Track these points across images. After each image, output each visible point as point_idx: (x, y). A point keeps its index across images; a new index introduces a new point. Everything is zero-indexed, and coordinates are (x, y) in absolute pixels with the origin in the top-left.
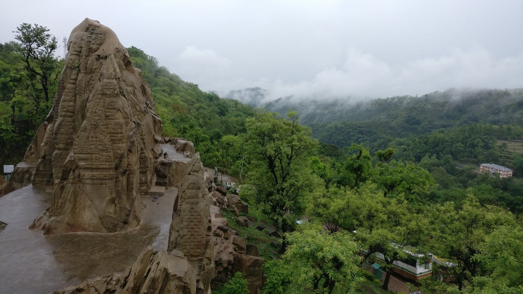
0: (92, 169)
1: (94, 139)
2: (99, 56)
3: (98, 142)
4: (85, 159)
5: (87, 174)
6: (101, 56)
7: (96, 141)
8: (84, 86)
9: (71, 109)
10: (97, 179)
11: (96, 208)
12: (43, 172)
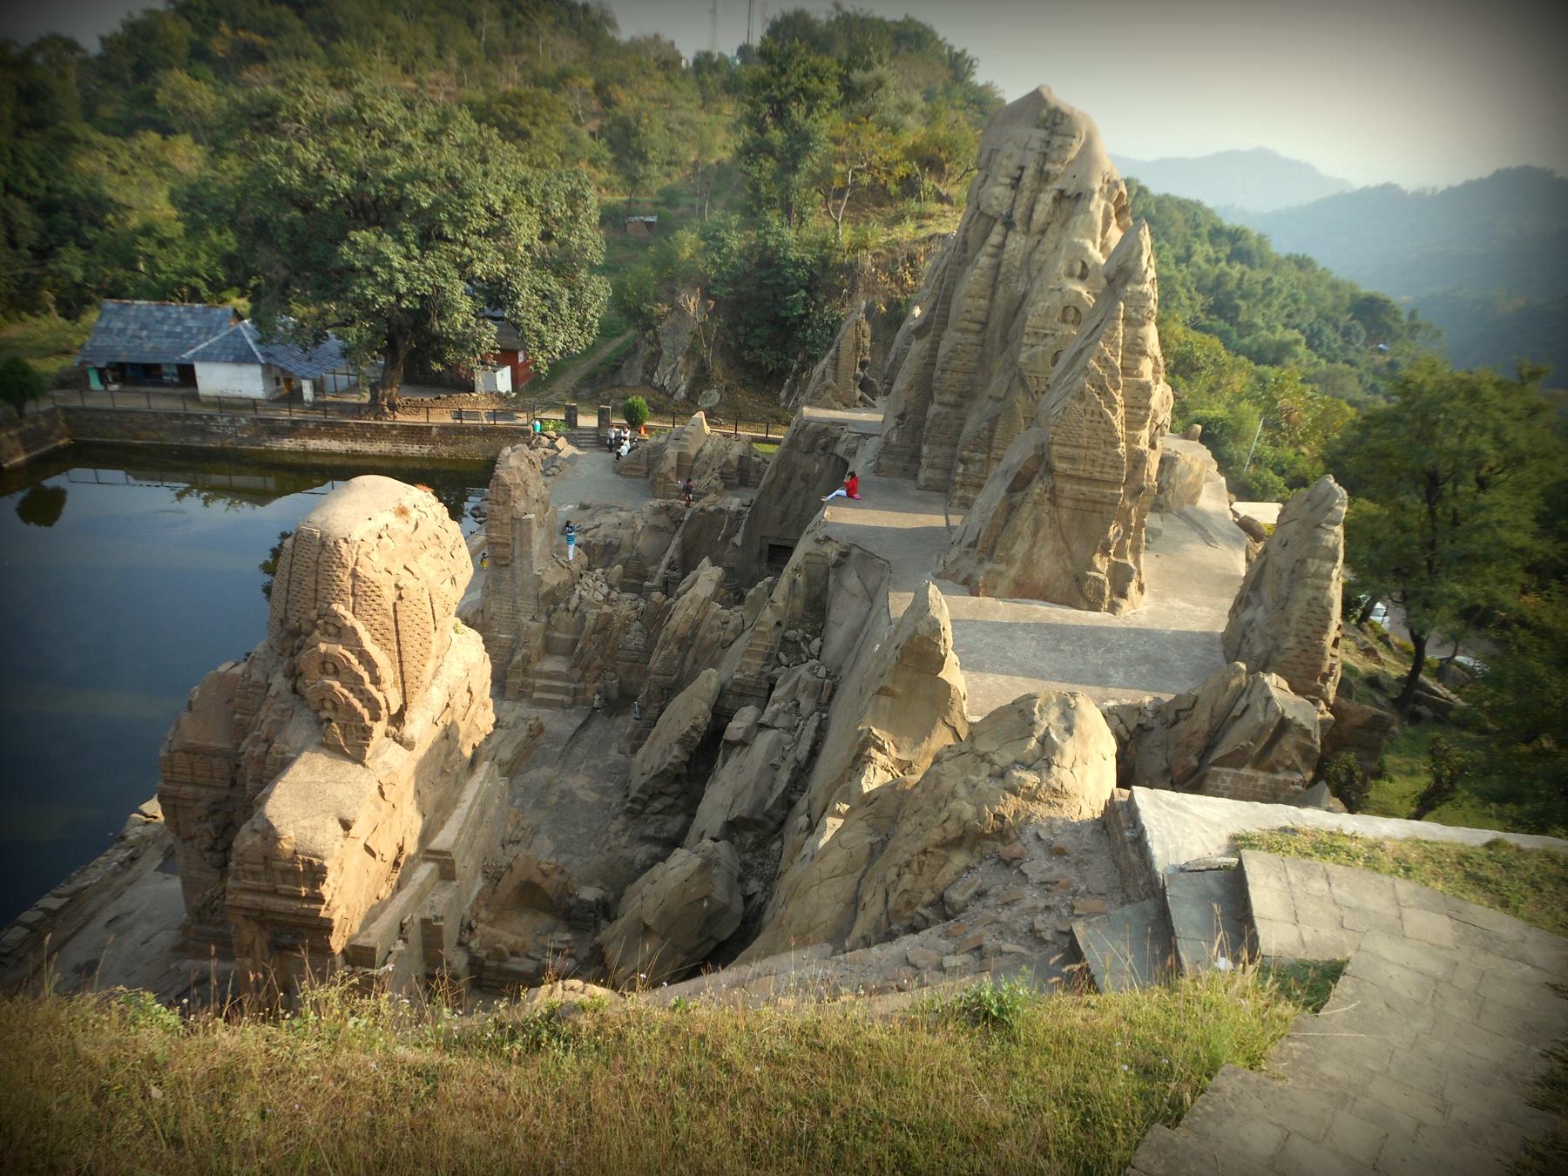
0: (1079, 480)
1: (1096, 418)
2: (1061, 192)
5: (1068, 488)
6: (1068, 193)
8: (1017, 264)
9: (980, 316)
11: (1071, 558)
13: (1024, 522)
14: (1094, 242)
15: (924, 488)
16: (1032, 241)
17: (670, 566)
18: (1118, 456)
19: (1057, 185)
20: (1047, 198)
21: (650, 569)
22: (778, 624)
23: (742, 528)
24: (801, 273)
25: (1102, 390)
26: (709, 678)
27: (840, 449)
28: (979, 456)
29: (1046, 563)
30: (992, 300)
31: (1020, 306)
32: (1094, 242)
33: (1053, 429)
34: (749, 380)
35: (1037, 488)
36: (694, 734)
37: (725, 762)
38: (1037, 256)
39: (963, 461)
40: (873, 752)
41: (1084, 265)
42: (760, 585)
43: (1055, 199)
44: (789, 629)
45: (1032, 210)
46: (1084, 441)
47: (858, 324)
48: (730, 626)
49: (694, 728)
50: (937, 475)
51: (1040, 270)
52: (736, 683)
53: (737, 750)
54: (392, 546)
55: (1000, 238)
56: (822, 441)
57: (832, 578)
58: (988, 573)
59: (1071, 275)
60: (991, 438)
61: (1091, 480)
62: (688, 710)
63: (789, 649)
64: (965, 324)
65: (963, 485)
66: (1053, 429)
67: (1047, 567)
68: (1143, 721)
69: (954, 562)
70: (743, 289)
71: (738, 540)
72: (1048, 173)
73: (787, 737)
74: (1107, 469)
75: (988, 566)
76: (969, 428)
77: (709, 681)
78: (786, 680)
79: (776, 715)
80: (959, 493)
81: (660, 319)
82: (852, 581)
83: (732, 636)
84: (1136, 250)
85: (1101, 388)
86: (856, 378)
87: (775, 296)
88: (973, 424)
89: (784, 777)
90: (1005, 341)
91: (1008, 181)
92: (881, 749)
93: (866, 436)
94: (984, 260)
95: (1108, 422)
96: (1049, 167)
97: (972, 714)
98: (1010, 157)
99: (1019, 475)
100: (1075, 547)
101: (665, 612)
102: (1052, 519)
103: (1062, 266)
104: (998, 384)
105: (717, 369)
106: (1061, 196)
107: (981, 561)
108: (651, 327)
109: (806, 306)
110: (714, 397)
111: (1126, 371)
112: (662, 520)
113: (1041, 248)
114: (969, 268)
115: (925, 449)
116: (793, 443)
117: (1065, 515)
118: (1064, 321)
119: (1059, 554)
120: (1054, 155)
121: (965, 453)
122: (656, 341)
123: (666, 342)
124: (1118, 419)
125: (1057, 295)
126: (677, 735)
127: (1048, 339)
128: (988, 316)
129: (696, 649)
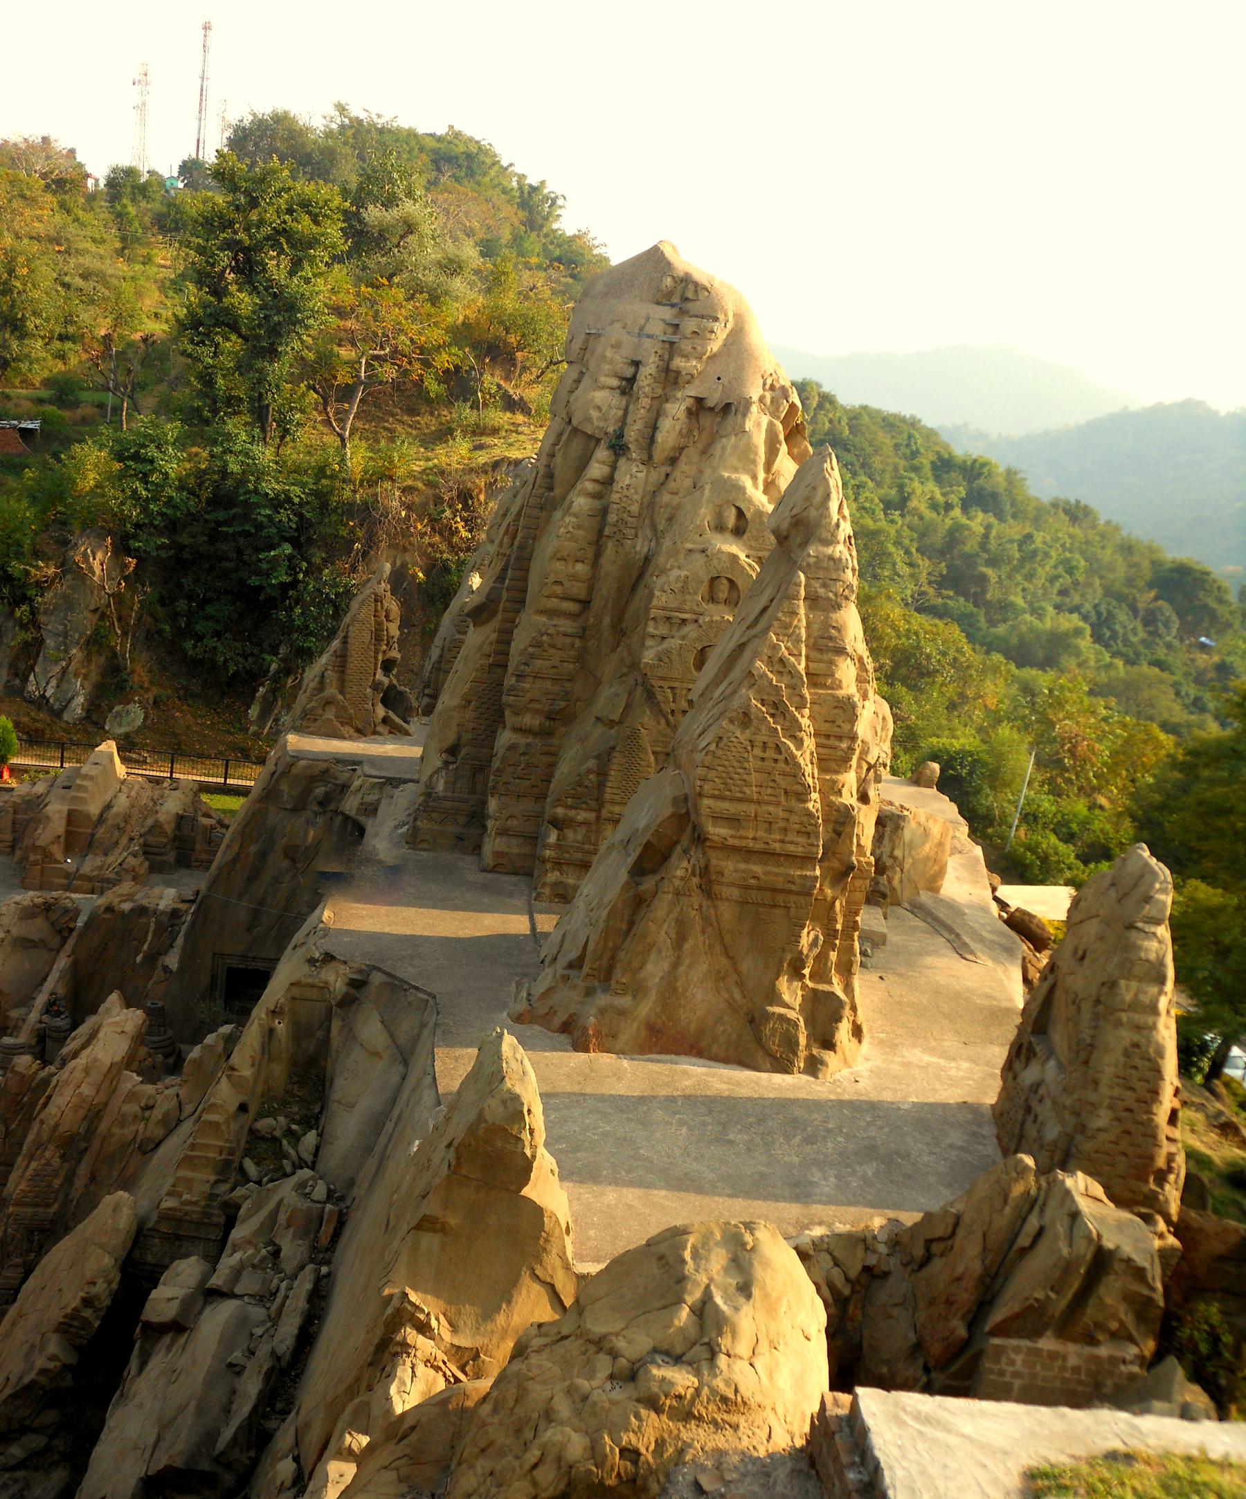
0: (747, 854)
1: (770, 754)
2: (699, 401)
3: (781, 765)
4: (733, 821)
5: (730, 867)
6: (710, 403)
7: (776, 761)
8: (635, 508)
9: (579, 590)
10: (759, 889)
11: (740, 984)
12: (448, 804)
13: (659, 924)
14: (754, 478)
15: (493, 870)
16: (656, 475)
17: (51, 1008)
18: (809, 814)
19: (693, 391)
20: (677, 410)
21: (14, 1014)
22: (243, 1108)
23: (180, 941)
24: (283, 516)
25: (778, 709)
26: (117, 1208)
27: (350, 805)
28: (582, 816)
29: (699, 996)
30: (595, 563)
31: (640, 576)
32: (754, 478)
33: (700, 771)
34: (196, 689)
35: (680, 868)
36: (87, 1313)
37: (143, 1364)
38: (665, 497)
39: (556, 823)
40: (411, 1335)
41: (740, 514)
42: (210, 1039)
43: (689, 412)
44: (260, 1115)
45: (655, 428)
46: (752, 792)
47: (378, 599)
48: (157, 1114)
49: (87, 1302)
50: (514, 847)
51: (670, 519)
52: (166, 1216)
53: (167, 1339)
55: (605, 470)
56: (320, 791)
57: (336, 1025)
58: (602, 1012)
59: (720, 528)
60: (601, 785)
61: (767, 855)
62: (77, 1268)
63: (262, 1151)
64: (553, 603)
65: (558, 864)
66: (700, 771)
67: (701, 999)
69: (545, 995)
70: (184, 539)
71: (172, 960)
72: (678, 373)
73: (257, 1313)
74: (792, 837)
75: (603, 999)
76: (564, 770)
77: (116, 1213)
78: (258, 1207)
79: (237, 1273)
80: (552, 877)
81: (42, 587)
82: (371, 1029)
83: (159, 1132)
84: (820, 491)
85: (775, 706)
86: (376, 686)
87: (240, 552)
88: (572, 761)
89: (251, 1386)
90: (619, 631)
91: (615, 382)
92: (424, 1328)
93: (393, 782)
94: (580, 502)
95: (791, 761)
96: (678, 363)
97: (581, 1257)
98: (617, 346)
99: (648, 845)
100: (746, 965)
101: (40, 1090)
102: (706, 920)
103: (705, 515)
104: (609, 699)
105: (140, 668)
106: (699, 407)
107: (589, 992)
108: (25, 599)
109: (292, 569)
110: (134, 716)
111: (815, 679)
112: (38, 928)
113: (672, 485)
114: (558, 514)
115: (493, 804)
116: (270, 794)
117: (727, 912)
118: (712, 599)
119: (720, 977)
120: (686, 346)
121: (560, 811)
122: (33, 622)
123: (51, 625)
124: (806, 755)
125: (699, 559)
126: (56, 1315)
127: (687, 629)
128: (591, 588)
129: (98, 1161)
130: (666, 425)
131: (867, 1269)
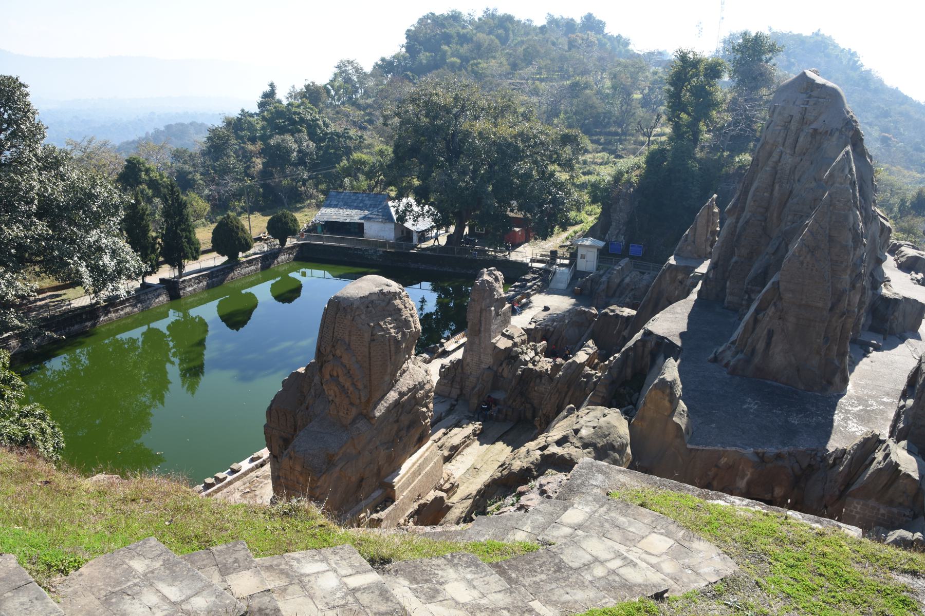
2: (815, 130)
19: (814, 126)
35: (771, 310)
54: (374, 311)
68: (813, 463)
115: (728, 283)
130: (801, 139)
131: (810, 466)
